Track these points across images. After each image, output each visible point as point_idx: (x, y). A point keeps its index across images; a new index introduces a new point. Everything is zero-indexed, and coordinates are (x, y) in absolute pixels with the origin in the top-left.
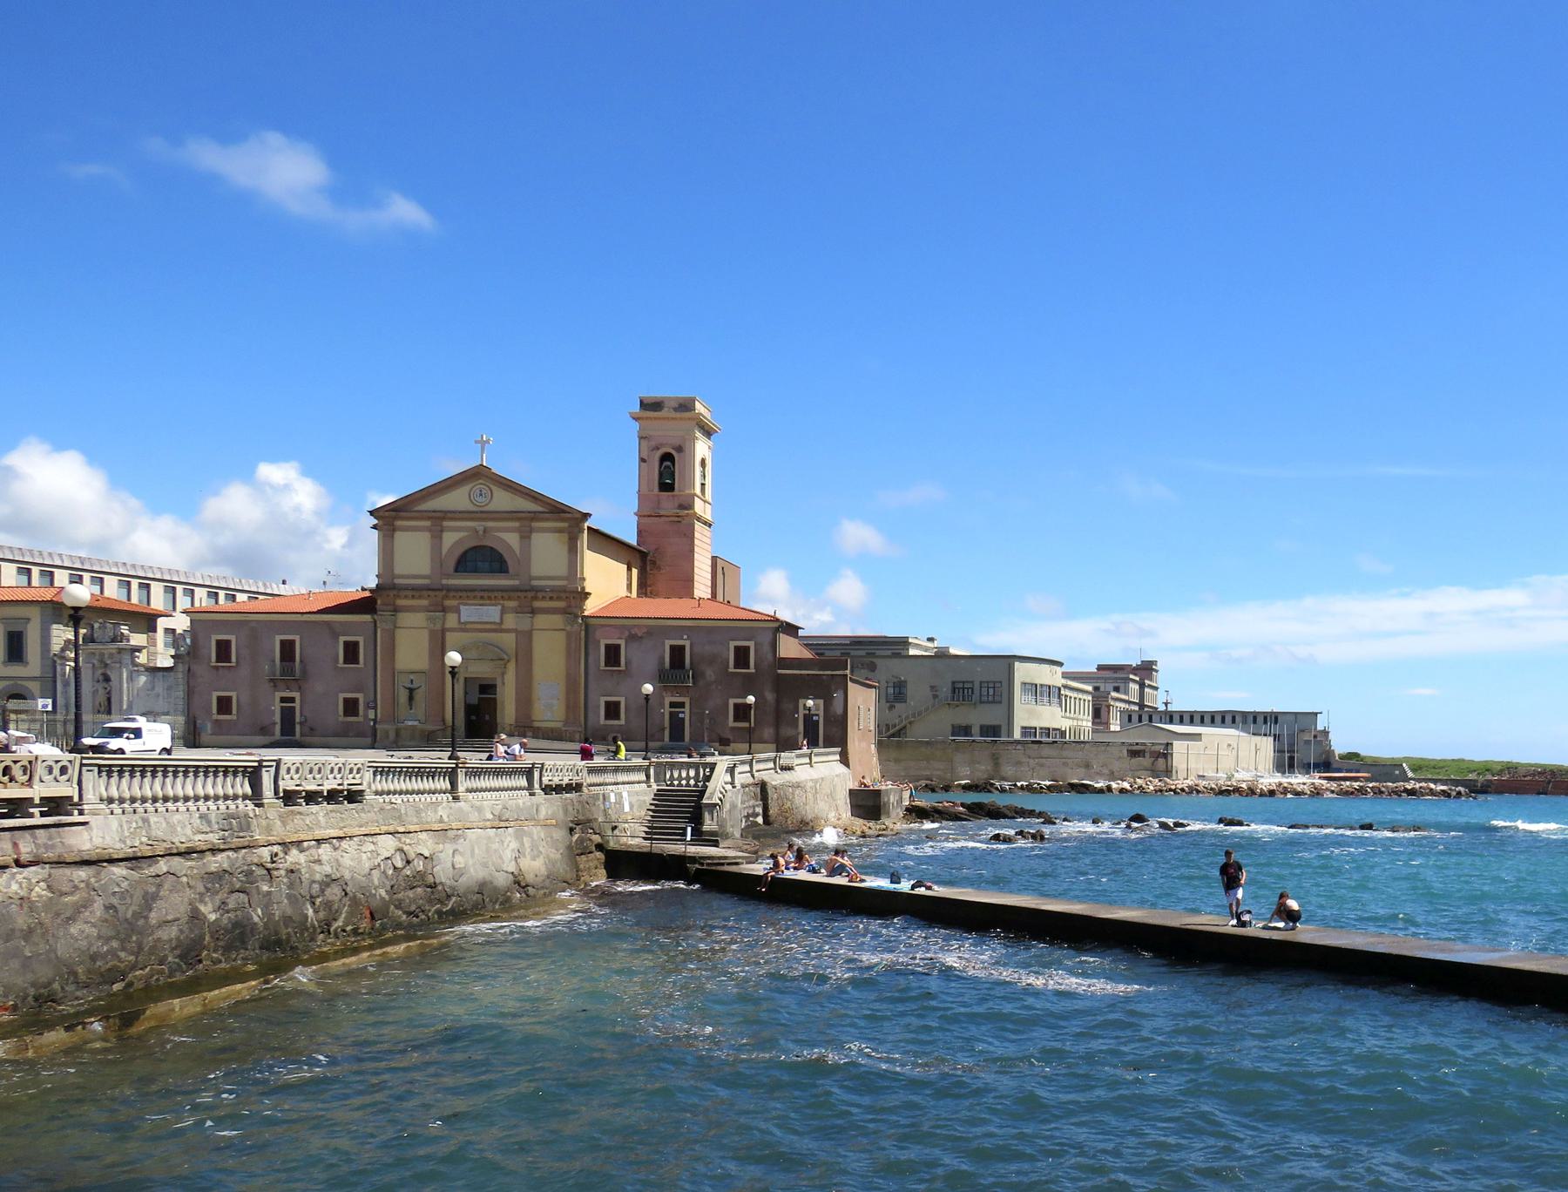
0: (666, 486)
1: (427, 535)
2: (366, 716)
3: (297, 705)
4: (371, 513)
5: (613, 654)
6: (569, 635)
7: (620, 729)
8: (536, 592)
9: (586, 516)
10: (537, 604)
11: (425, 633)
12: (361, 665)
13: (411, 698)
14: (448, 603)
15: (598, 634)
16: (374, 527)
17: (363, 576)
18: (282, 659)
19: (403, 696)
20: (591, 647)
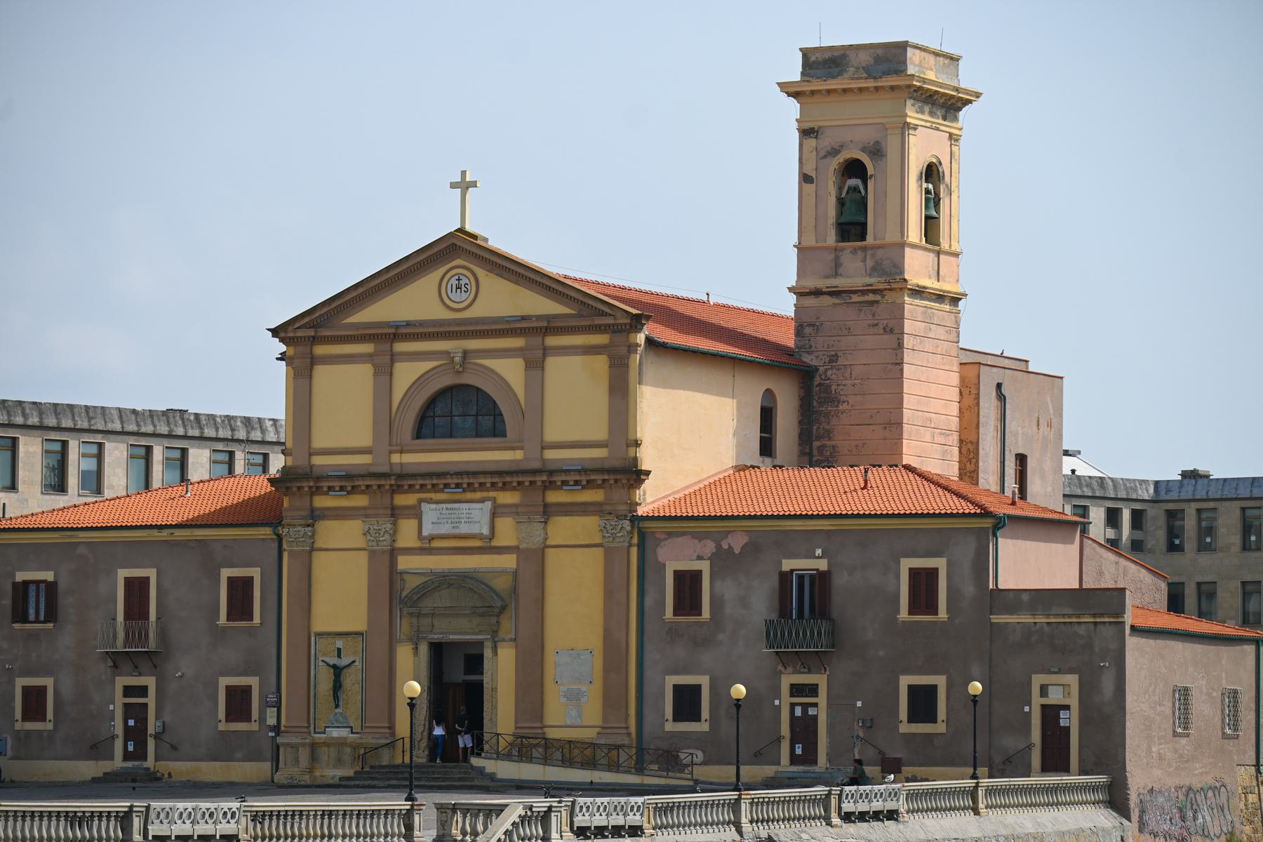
0: (852, 226)
1: (366, 370)
2: (262, 719)
3: (151, 700)
4: (275, 332)
7: (698, 741)
10: (554, 497)
11: (363, 558)
12: (257, 619)
13: (337, 686)
14: (402, 500)
15: (663, 553)
16: (282, 357)
18: (128, 616)
20: (650, 575)
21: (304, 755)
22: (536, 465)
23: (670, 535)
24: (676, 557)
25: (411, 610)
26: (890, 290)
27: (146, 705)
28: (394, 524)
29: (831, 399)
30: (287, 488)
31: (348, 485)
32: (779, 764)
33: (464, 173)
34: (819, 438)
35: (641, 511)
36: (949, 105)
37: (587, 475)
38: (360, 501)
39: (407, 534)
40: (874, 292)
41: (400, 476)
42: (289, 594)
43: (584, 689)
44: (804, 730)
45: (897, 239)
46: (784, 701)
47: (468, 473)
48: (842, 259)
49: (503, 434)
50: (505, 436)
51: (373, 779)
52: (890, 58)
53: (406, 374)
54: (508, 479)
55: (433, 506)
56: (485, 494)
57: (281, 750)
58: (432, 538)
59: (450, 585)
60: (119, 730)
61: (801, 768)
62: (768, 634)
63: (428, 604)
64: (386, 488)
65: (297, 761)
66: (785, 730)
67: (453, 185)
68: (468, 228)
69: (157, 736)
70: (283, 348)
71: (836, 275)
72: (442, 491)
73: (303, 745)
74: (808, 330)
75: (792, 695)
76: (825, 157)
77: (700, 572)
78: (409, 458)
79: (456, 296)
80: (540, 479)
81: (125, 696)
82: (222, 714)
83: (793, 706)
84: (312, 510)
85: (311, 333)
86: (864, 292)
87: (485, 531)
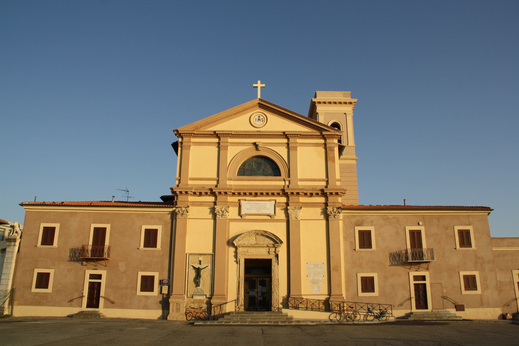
19: (192, 274)
27: (100, 283)
43: (321, 279)
49: (280, 175)
75: (414, 280)
87: (272, 213)
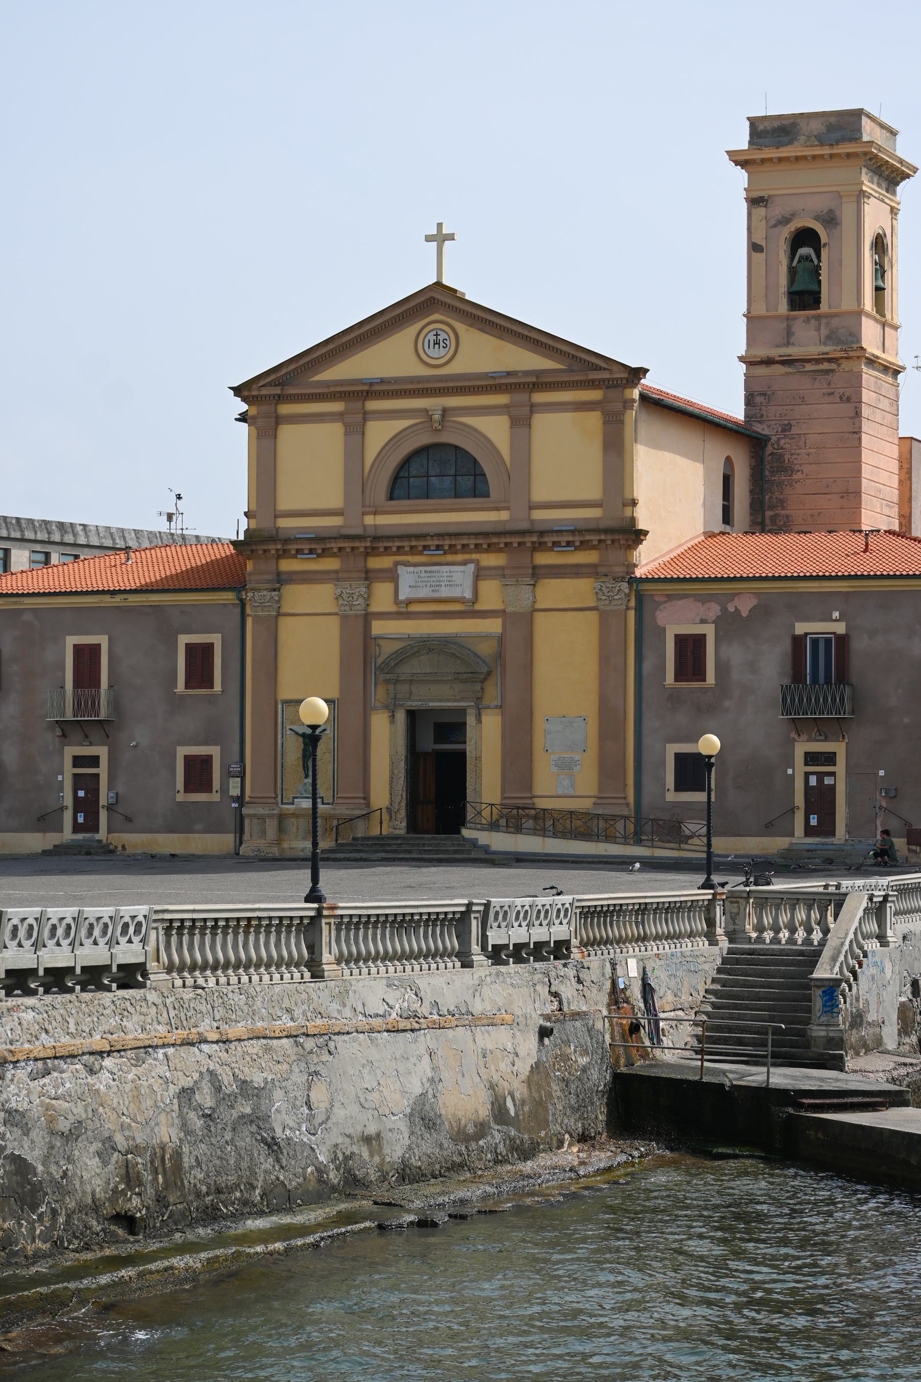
0: (804, 297)
1: (337, 429)
2: (224, 790)
3: (103, 771)
4: (238, 391)
5: (690, 652)
6: (604, 617)
8: (540, 538)
9: (639, 373)
10: (543, 559)
11: (334, 624)
12: (218, 687)
14: (375, 563)
15: (662, 617)
16: (243, 418)
17: (220, 515)
18: (77, 684)
21: (271, 827)
22: (525, 526)
23: (670, 598)
24: (677, 621)
25: (388, 676)
26: (847, 358)
28: (368, 588)
29: (784, 467)
30: (252, 551)
31: (319, 547)
32: (793, 835)
33: (440, 226)
34: (771, 508)
35: (639, 573)
36: (892, 175)
37: (580, 536)
38: (331, 564)
39: (382, 597)
40: (830, 360)
41: (376, 539)
42: (253, 660)
43: (577, 757)
44: (820, 800)
45: (854, 307)
46: (799, 768)
47: (450, 535)
48: (794, 329)
50: (488, 496)
51: (359, 851)
52: (843, 127)
53: (379, 434)
54: (495, 540)
55: (411, 569)
56: (467, 557)
57: (247, 822)
58: (409, 602)
59: (430, 650)
60: (68, 801)
61: (817, 840)
62: (784, 700)
63: (406, 670)
64: (357, 551)
65: (264, 832)
66: (799, 799)
67: (429, 239)
68: (446, 282)
69: (110, 808)
70: (244, 407)
71: (788, 344)
72: (421, 553)
73: (271, 816)
74: (759, 399)
75: (806, 764)
76: (775, 226)
77: (704, 636)
78: (383, 520)
79: (434, 352)
80: (528, 540)
81: (75, 766)
82: (180, 785)
83: (807, 775)
84: (279, 574)
85: (277, 391)
86: (818, 361)
87: (468, 594)
